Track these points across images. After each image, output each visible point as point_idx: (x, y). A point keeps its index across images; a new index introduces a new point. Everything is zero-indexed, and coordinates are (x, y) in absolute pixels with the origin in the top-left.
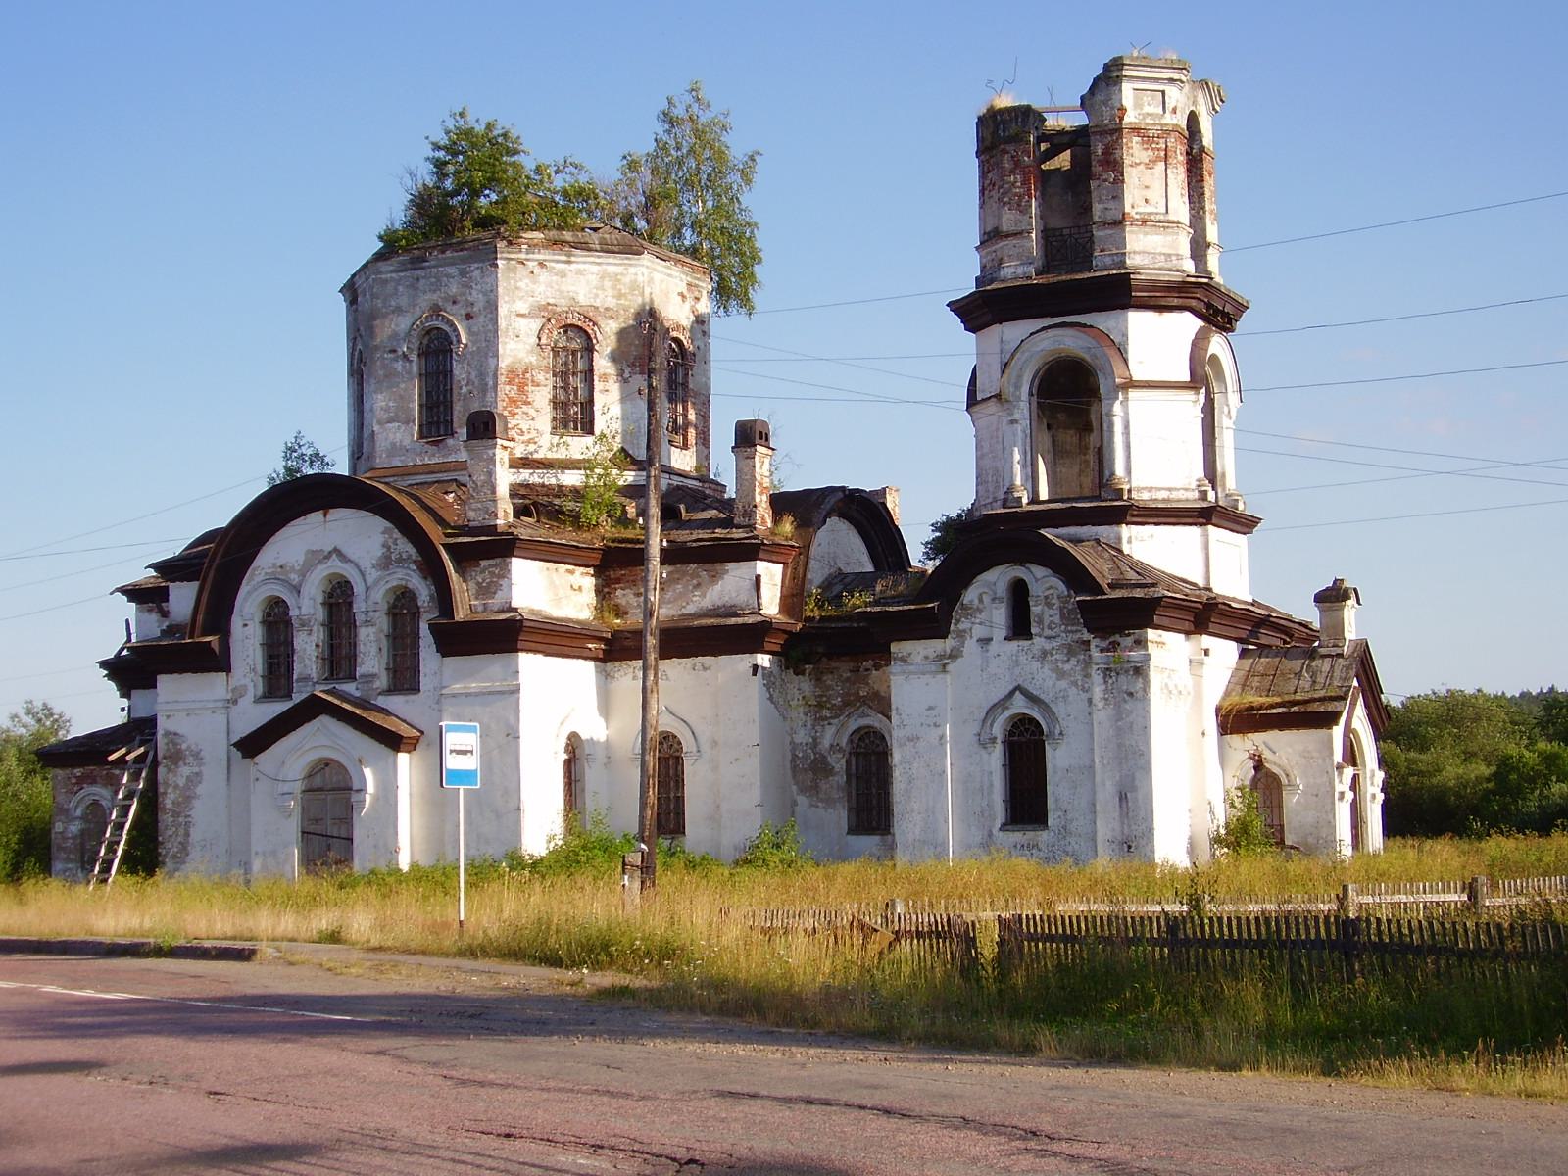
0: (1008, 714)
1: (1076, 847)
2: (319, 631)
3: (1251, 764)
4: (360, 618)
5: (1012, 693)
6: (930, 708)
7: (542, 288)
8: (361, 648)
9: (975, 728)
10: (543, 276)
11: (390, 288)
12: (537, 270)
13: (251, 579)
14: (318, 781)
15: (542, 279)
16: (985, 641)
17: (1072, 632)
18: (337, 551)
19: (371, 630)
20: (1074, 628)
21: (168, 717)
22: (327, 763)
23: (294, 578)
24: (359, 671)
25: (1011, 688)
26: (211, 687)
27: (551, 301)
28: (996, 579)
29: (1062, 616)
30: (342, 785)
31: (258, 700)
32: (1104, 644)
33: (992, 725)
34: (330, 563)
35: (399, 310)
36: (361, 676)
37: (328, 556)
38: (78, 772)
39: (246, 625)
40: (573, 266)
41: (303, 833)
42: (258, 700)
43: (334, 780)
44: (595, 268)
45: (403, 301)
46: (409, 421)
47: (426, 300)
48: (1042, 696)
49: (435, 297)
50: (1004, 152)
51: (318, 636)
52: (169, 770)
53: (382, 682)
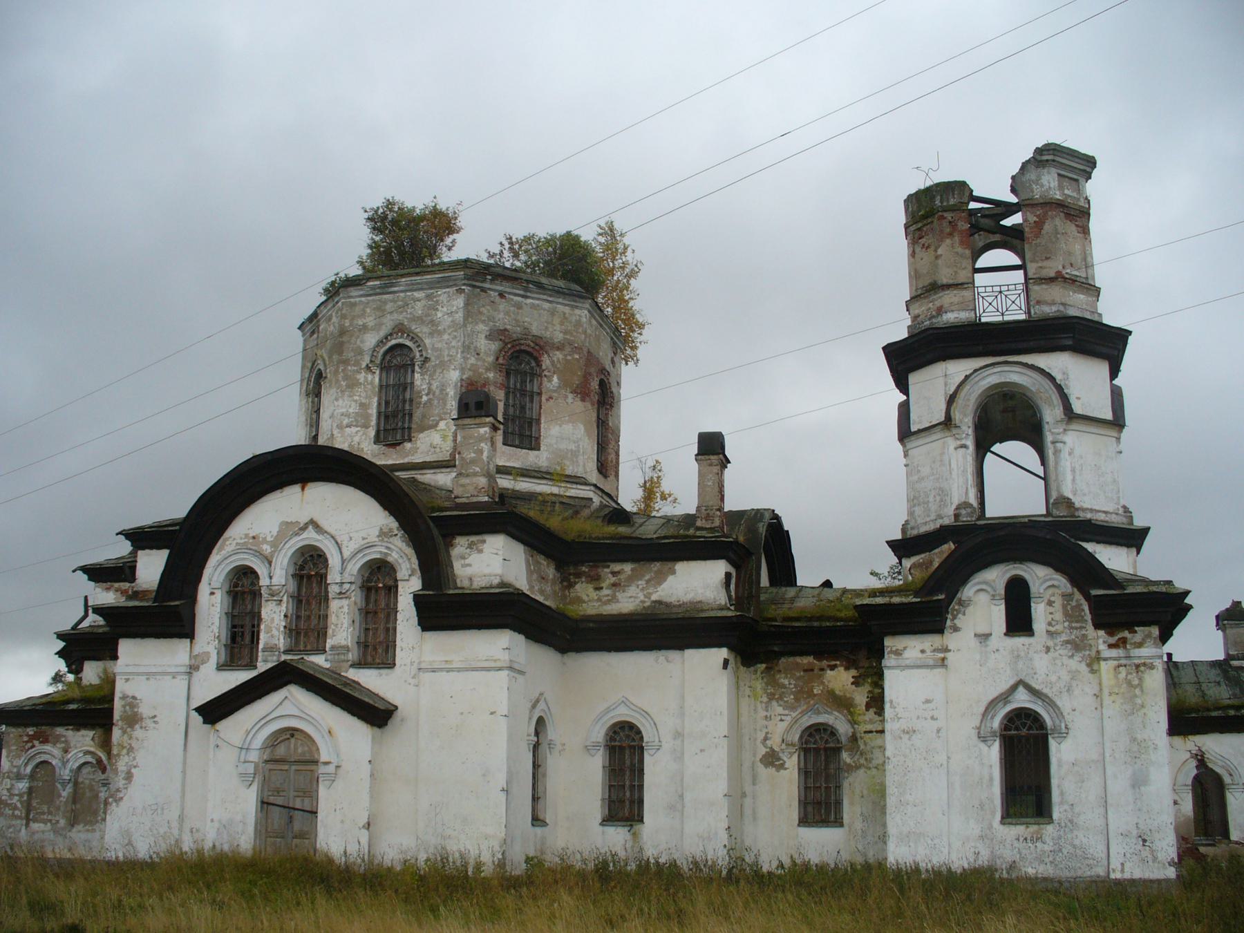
0: (1009, 708)
1: (1085, 840)
2: (288, 602)
3: (1194, 763)
4: (333, 590)
5: (1014, 688)
6: (928, 701)
7: (501, 316)
8: (332, 619)
9: (976, 721)
10: (503, 305)
11: (358, 309)
12: (498, 299)
13: (220, 550)
14: (281, 751)
15: (501, 307)
16: (984, 637)
17: (1076, 628)
18: (313, 523)
19: (345, 602)
20: (1078, 625)
21: (127, 680)
22: (292, 732)
23: (267, 549)
24: (329, 643)
25: (1012, 682)
26: (174, 653)
27: (508, 327)
28: (996, 576)
29: (1066, 614)
30: (308, 757)
31: (221, 667)
32: (1113, 640)
33: (992, 718)
34: (305, 535)
35: (365, 328)
36: (333, 648)
37: (304, 528)
38: (31, 731)
39: (212, 593)
40: (529, 301)
41: (263, 802)
42: (221, 667)
43: (300, 750)
44: (547, 305)
45: (370, 321)
46: (366, 426)
47: (388, 324)
48: (1046, 691)
49: (400, 317)
50: (942, 218)
51: (287, 608)
52: (124, 732)
53: (352, 656)
